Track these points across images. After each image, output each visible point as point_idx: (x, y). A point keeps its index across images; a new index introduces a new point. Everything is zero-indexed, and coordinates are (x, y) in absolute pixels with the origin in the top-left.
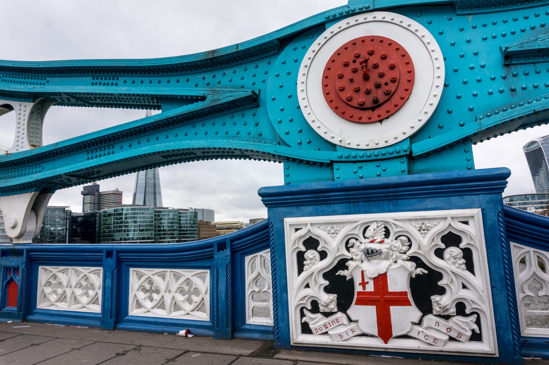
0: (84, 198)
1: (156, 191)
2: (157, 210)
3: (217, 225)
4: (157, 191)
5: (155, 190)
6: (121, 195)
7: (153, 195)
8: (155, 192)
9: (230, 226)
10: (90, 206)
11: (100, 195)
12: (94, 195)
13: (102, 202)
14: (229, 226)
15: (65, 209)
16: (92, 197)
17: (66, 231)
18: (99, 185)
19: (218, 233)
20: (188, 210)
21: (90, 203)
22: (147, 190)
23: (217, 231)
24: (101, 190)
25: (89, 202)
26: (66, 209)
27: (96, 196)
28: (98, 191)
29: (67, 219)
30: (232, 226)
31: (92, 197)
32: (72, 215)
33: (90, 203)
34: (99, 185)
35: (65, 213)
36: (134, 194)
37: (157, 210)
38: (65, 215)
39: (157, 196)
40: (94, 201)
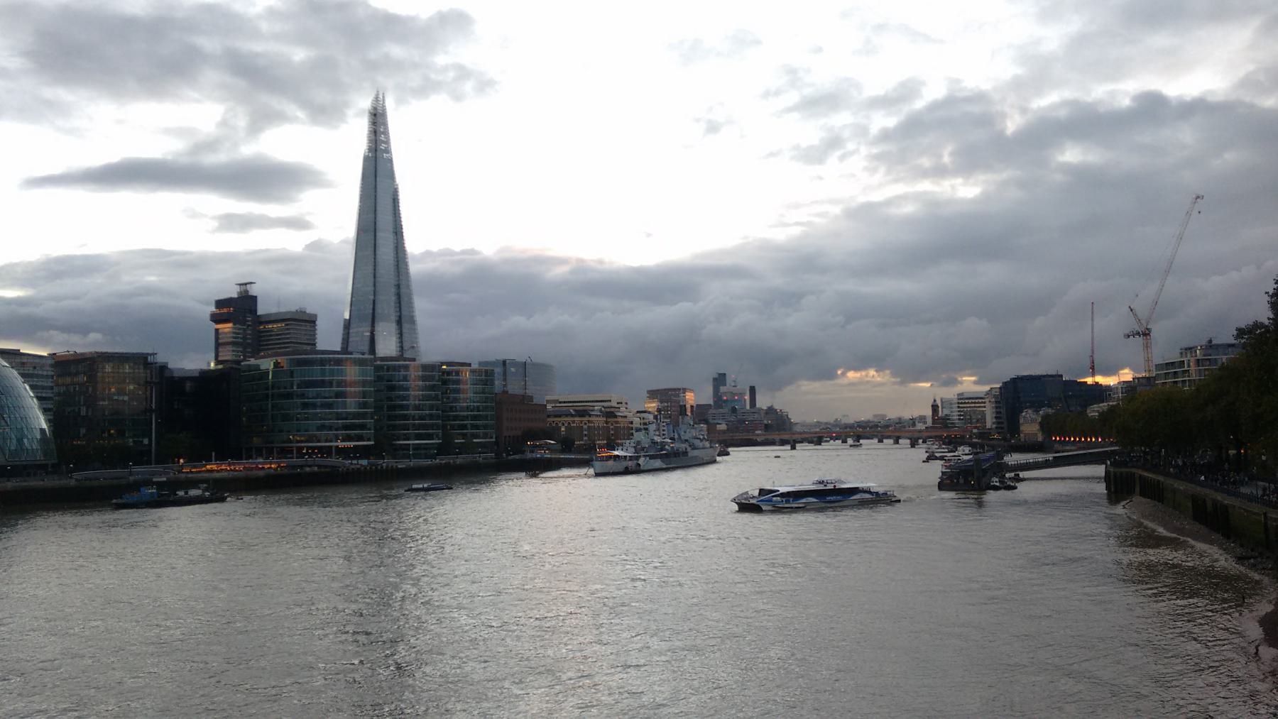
3: (549, 407)
6: (314, 322)
8: (400, 317)
10: (233, 351)
11: (261, 320)
12: (243, 322)
13: (264, 341)
15: (146, 358)
18: (256, 297)
19: (554, 425)
21: (233, 344)
22: (378, 311)
23: (549, 419)
25: (232, 340)
27: (249, 326)
31: (240, 329)
32: (167, 374)
33: (233, 344)
34: (256, 297)
39: (406, 326)
40: (245, 338)
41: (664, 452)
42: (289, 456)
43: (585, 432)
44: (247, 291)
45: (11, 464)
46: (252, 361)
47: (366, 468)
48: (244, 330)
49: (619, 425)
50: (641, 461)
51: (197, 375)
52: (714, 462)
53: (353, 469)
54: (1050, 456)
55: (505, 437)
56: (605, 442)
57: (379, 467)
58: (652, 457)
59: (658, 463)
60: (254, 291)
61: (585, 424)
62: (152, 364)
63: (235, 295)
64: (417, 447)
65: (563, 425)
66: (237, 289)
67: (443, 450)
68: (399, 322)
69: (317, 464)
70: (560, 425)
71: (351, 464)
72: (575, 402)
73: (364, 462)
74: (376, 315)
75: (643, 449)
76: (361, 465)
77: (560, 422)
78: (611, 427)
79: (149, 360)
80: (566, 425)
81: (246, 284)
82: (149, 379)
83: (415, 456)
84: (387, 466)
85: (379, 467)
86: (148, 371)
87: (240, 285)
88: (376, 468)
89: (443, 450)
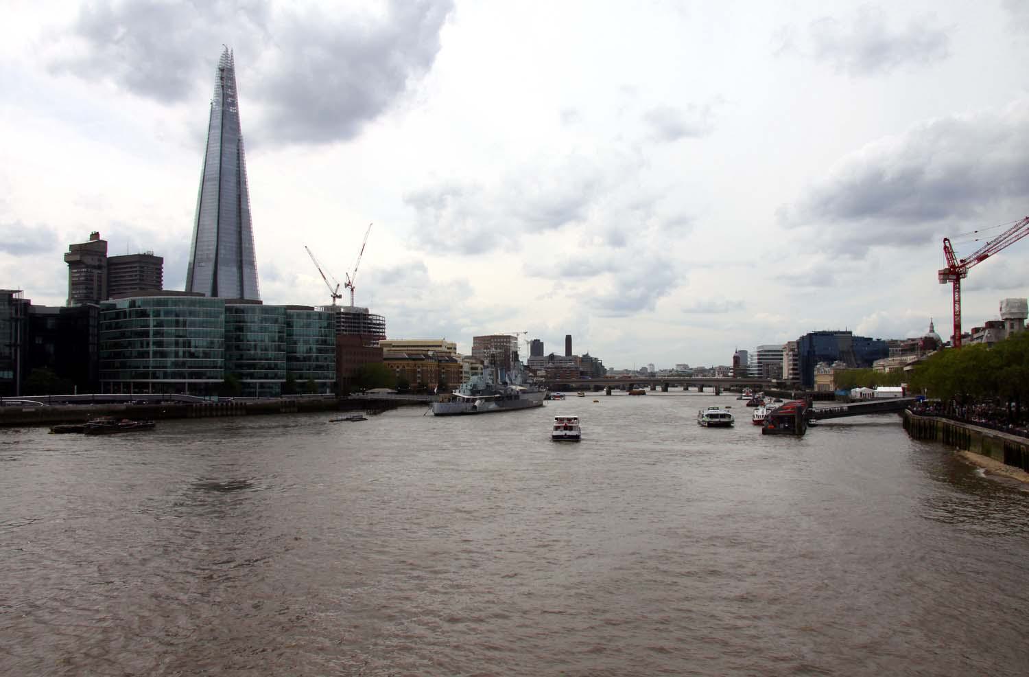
2: (235, 305)
15: (12, 295)
24: (111, 253)
26: (15, 296)
32: (30, 311)
35: (14, 308)
37: (235, 305)
38: (13, 312)
39: (246, 270)
41: (498, 395)
42: (145, 391)
43: (419, 375)
46: (111, 301)
47: (217, 405)
49: (449, 369)
50: (477, 403)
51: (58, 312)
52: (541, 406)
53: (206, 405)
54: (845, 406)
55: (345, 378)
57: (230, 404)
58: (487, 400)
59: (493, 406)
61: (419, 367)
64: (262, 385)
67: (287, 388)
68: (240, 268)
70: (395, 368)
71: (204, 400)
73: (215, 399)
74: (219, 260)
75: (478, 392)
76: (213, 402)
79: (14, 297)
80: (401, 367)
82: (14, 316)
83: (261, 395)
84: (237, 404)
85: (230, 404)
86: (14, 308)
88: (222, 405)
89: (287, 388)
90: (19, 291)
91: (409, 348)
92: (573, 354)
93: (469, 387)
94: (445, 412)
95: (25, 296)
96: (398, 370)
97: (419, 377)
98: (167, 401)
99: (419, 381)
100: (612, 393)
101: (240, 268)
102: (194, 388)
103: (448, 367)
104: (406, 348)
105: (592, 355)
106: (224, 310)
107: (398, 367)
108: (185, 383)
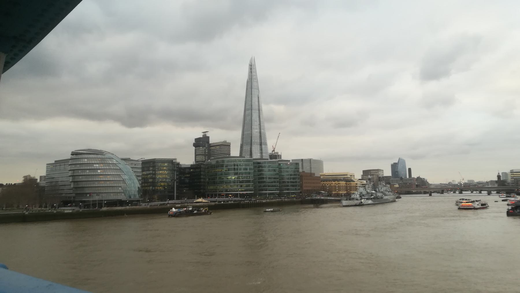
0: (195, 150)
1: (262, 141)
3: (322, 177)
4: (262, 141)
5: (261, 140)
7: (259, 146)
9: (337, 178)
11: (210, 146)
12: (204, 146)
14: (335, 178)
15: (173, 161)
16: (203, 149)
17: (174, 182)
18: (209, 137)
19: (324, 185)
20: (289, 161)
22: (253, 141)
23: (322, 183)
26: (174, 161)
27: (206, 148)
28: (208, 142)
29: (174, 170)
30: (339, 178)
31: (203, 149)
34: (209, 137)
36: (241, 144)
38: (173, 167)
39: (263, 146)
40: (205, 152)
44: (205, 135)
45: (128, 200)
48: (205, 149)
51: (190, 166)
52: (395, 201)
55: (304, 190)
56: (346, 192)
58: (367, 199)
59: (370, 202)
60: (208, 135)
61: (337, 185)
62: (174, 163)
63: (202, 137)
65: (328, 185)
66: (203, 134)
68: (261, 144)
69: (233, 200)
72: (332, 175)
77: (326, 184)
78: (348, 186)
81: (205, 132)
87: (203, 132)
89: (280, 195)
90: (175, 159)
91: (332, 176)
92: (413, 176)
93: (358, 194)
94: (347, 205)
95: (178, 161)
96: (328, 186)
97: (337, 189)
98: (231, 201)
99: (337, 191)
100: (432, 195)
101: (261, 144)
102: (242, 196)
103: (351, 184)
104: (331, 176)
105: (421, 177)
106: (253, 163)
107: (328, 185)
108: (238, 194)
